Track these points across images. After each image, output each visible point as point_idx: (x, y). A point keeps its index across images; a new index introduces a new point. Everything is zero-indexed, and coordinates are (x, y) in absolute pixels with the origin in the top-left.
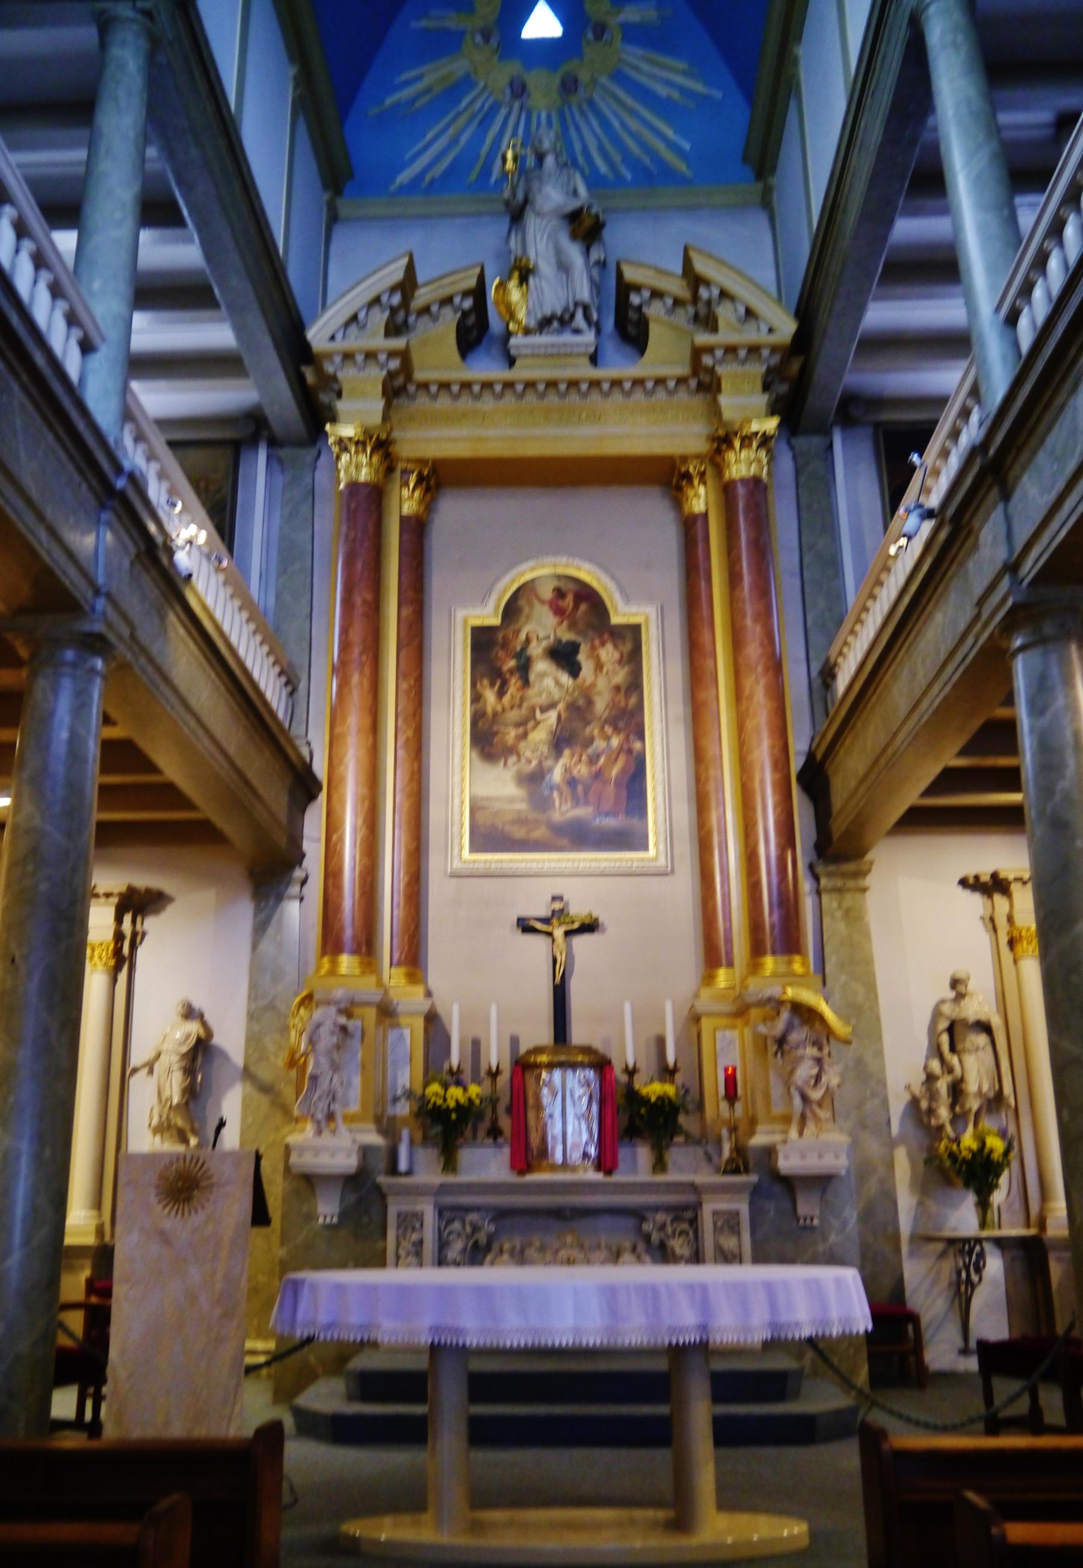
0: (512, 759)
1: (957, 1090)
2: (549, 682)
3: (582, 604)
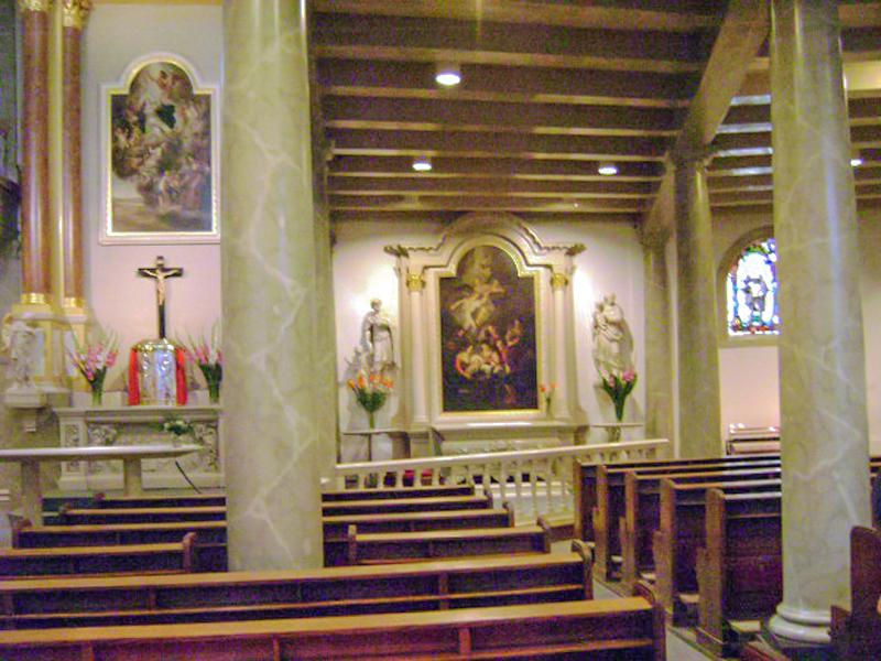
0: (135, 176)
1: (371, 357)
2: (157, 130)
3: (178, 81)
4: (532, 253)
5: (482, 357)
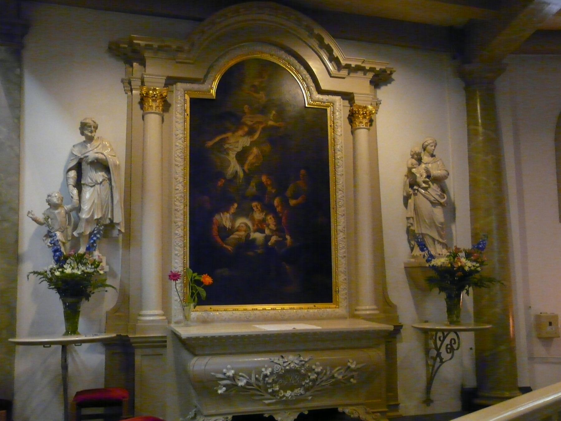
4: (316, 77)
5: (252, 219)
